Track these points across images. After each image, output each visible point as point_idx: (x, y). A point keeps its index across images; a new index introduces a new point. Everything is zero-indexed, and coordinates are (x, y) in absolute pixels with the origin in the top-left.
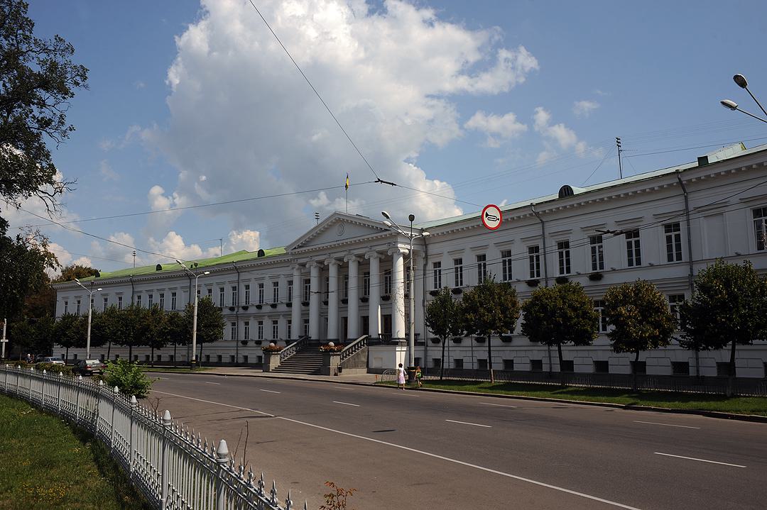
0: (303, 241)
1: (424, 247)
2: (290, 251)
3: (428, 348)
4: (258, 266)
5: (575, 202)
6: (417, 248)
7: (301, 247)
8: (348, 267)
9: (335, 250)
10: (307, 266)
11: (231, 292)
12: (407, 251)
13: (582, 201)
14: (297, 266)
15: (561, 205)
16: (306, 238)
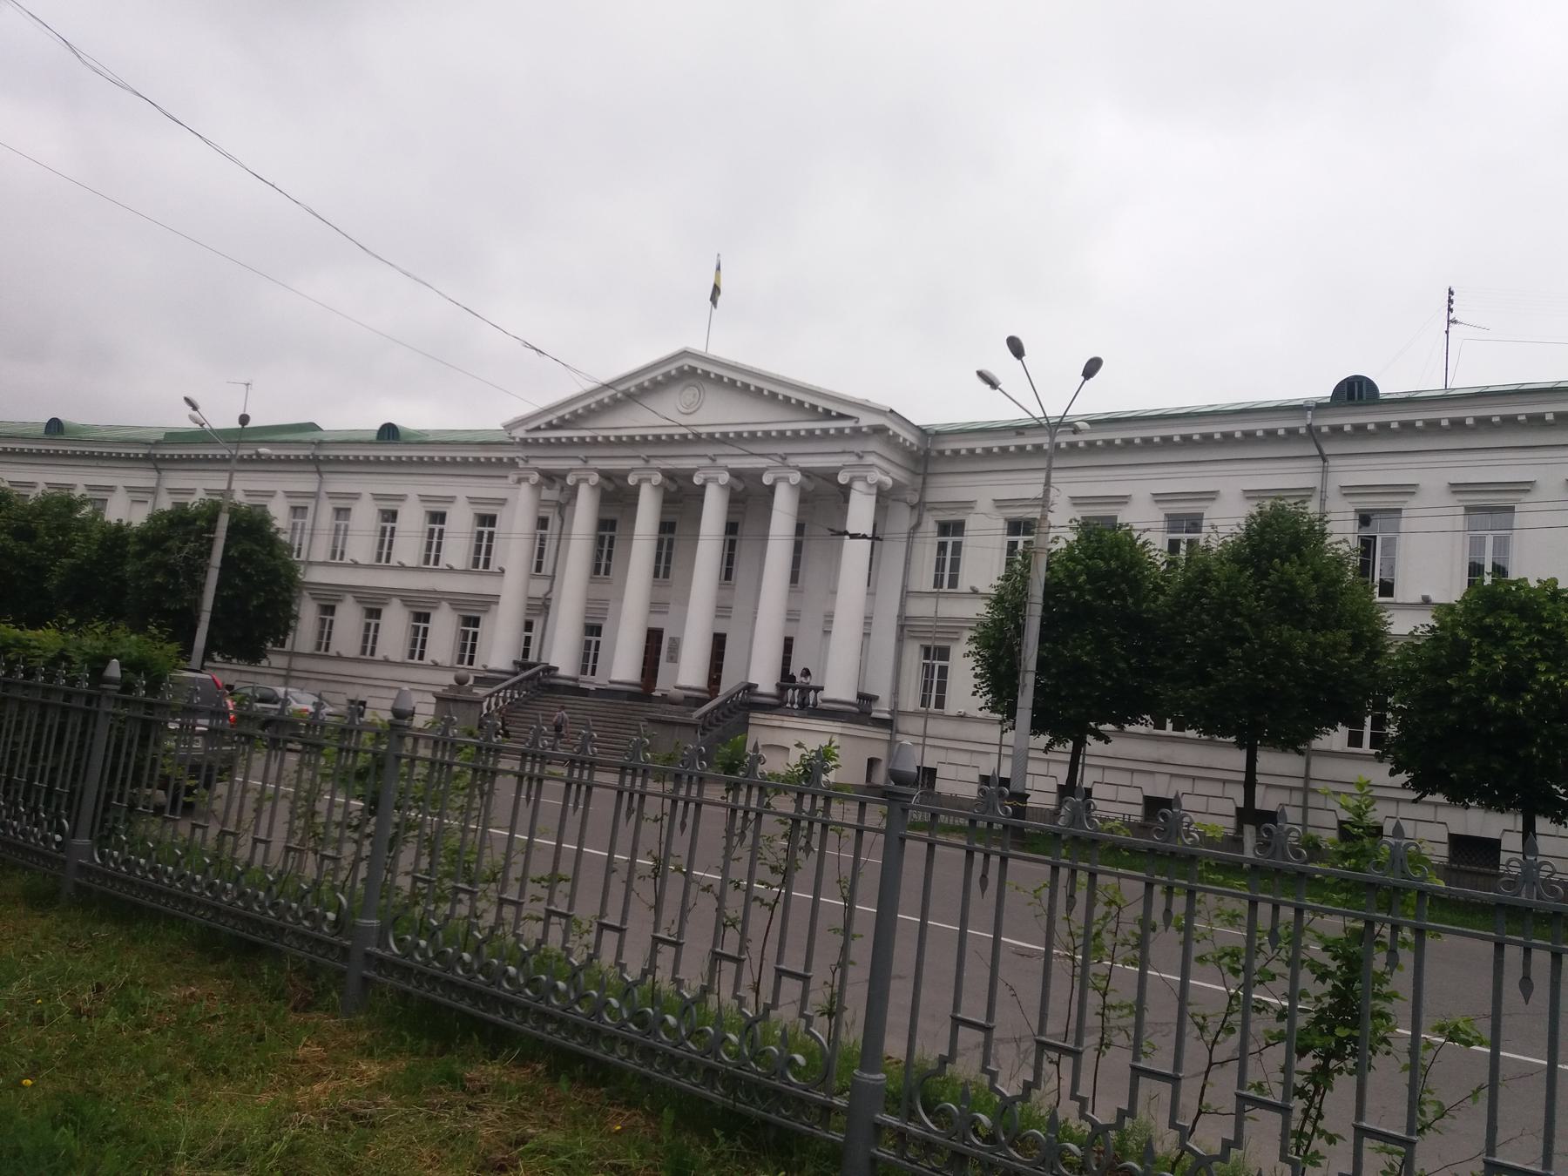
0: (565, 412)
1: (919, 480)
2: (519, 433)
3: (899, 737)
4: (377, 461)
5: (1370, 419)
6: (901, 476)
7: (551, 426)
8: (635, 505)
9: (607, 452)
10: (570, 480)
11: (1000, 541)
12: (889, 481)
13: (1394, 418)
14: (535, 477)
15: (1347, 420)
16: (579, 407)
